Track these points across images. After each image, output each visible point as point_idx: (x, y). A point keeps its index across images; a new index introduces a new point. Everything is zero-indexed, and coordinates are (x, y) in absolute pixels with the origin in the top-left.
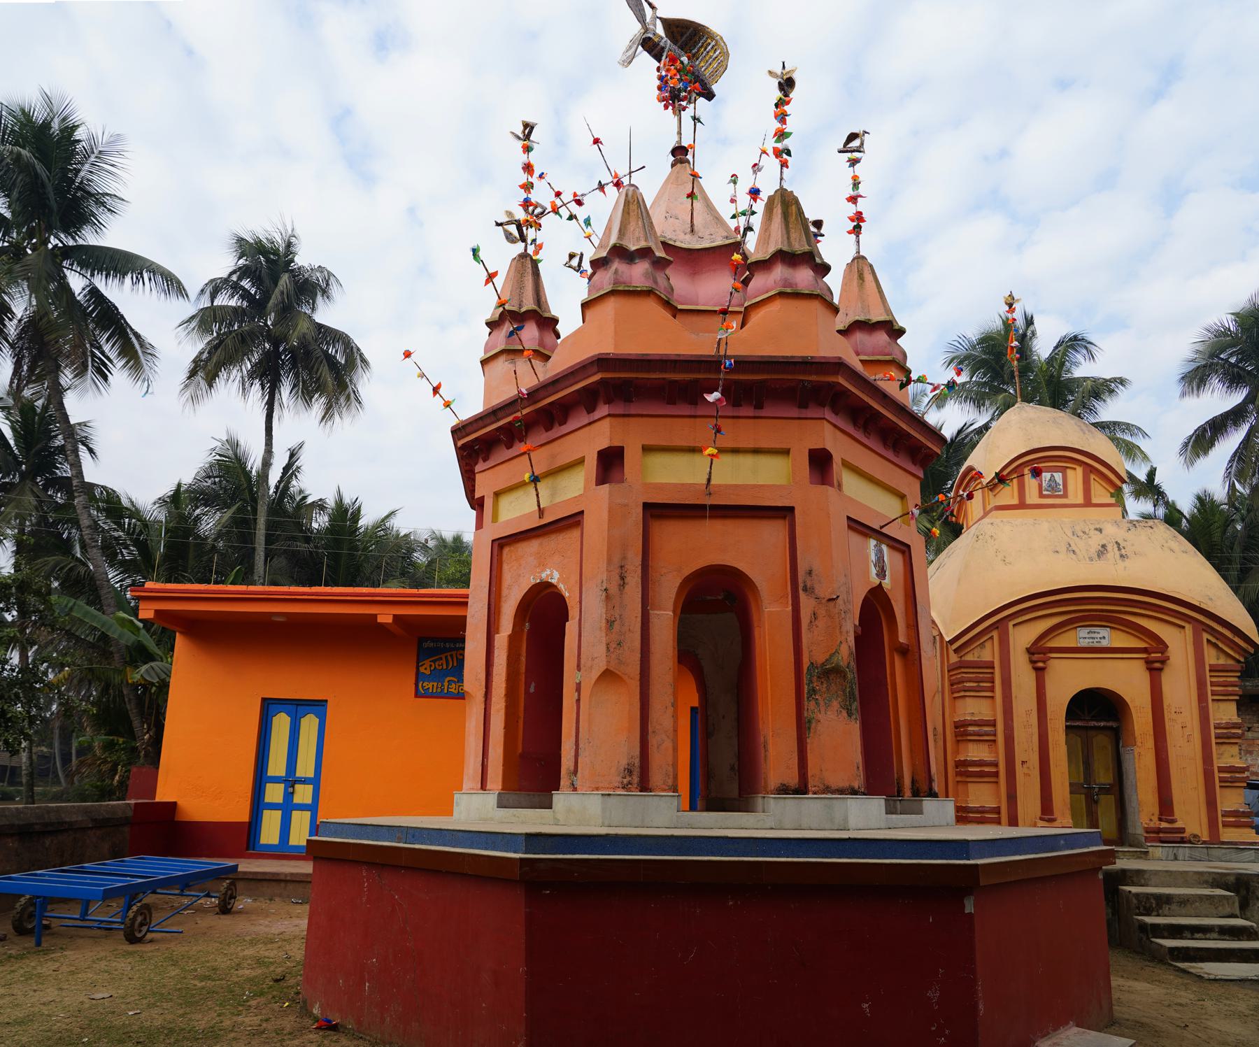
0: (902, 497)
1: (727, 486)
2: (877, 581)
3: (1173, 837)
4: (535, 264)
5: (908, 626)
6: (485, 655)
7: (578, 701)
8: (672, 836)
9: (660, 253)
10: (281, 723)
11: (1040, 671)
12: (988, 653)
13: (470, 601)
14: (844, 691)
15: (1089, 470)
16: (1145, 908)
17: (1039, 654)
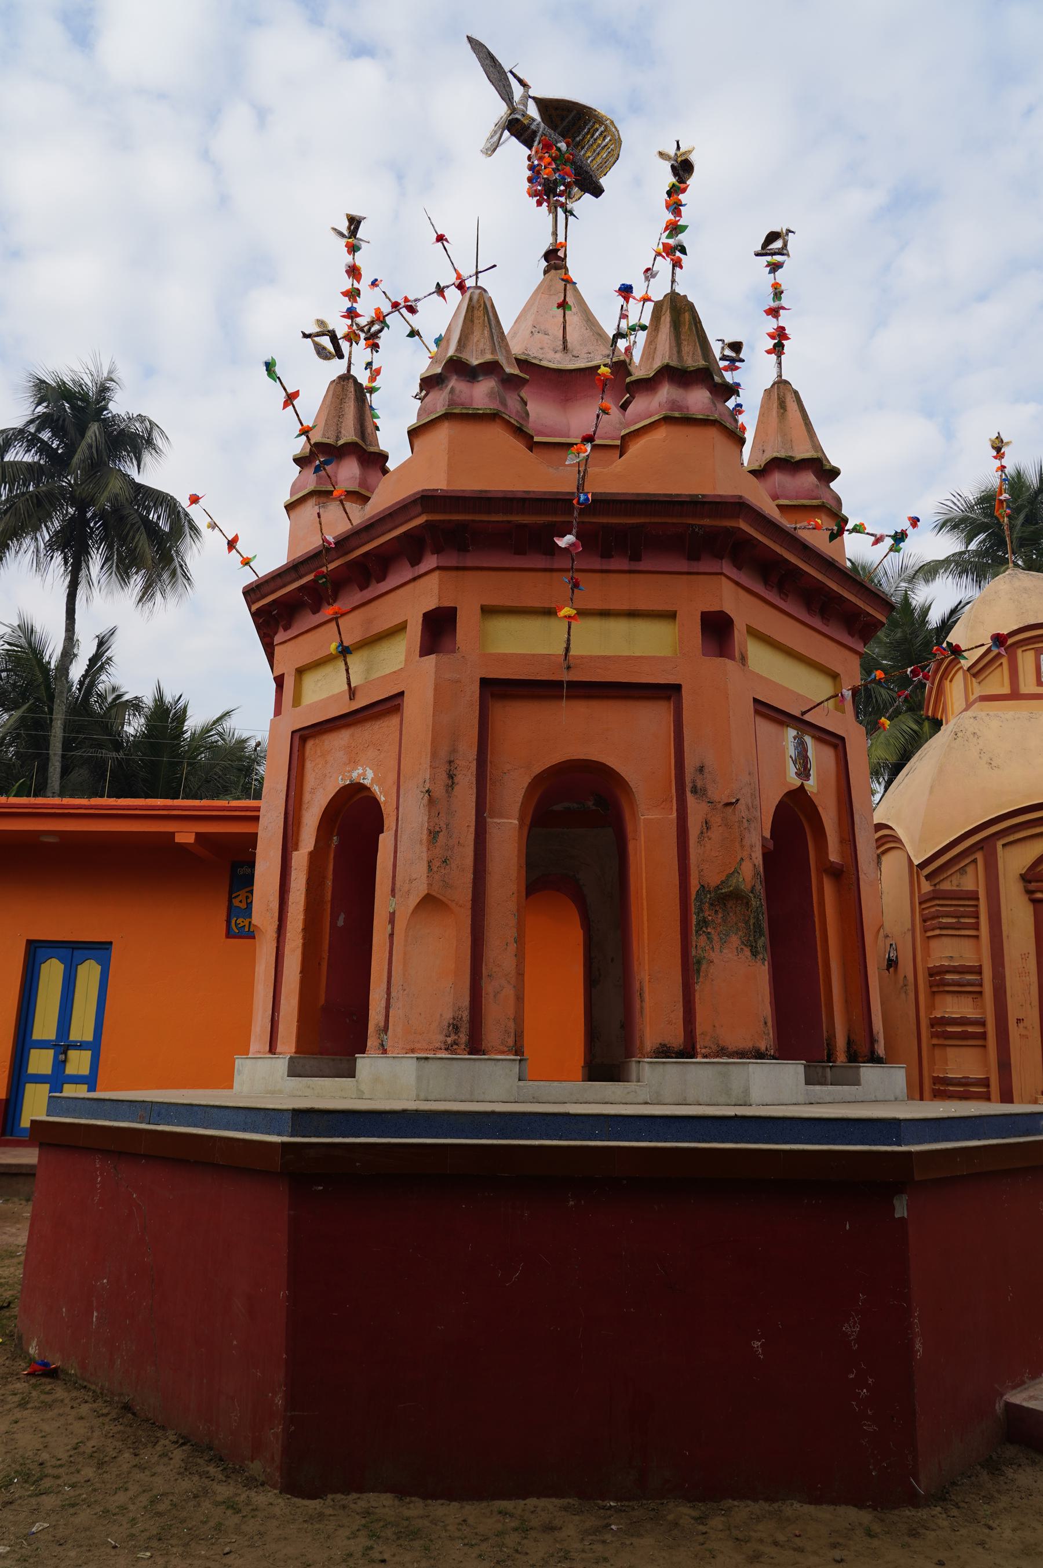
0: (834, 676)
1: (592, 658)
2: (797, 782)
4: (361, 393)
5: (842, 841)
6: (279, 881)
7: (392, 935)
8: (493, 1113)
9: (511, 369)
10: (52, 972)
13: (262, 813)
14: (747, 922)
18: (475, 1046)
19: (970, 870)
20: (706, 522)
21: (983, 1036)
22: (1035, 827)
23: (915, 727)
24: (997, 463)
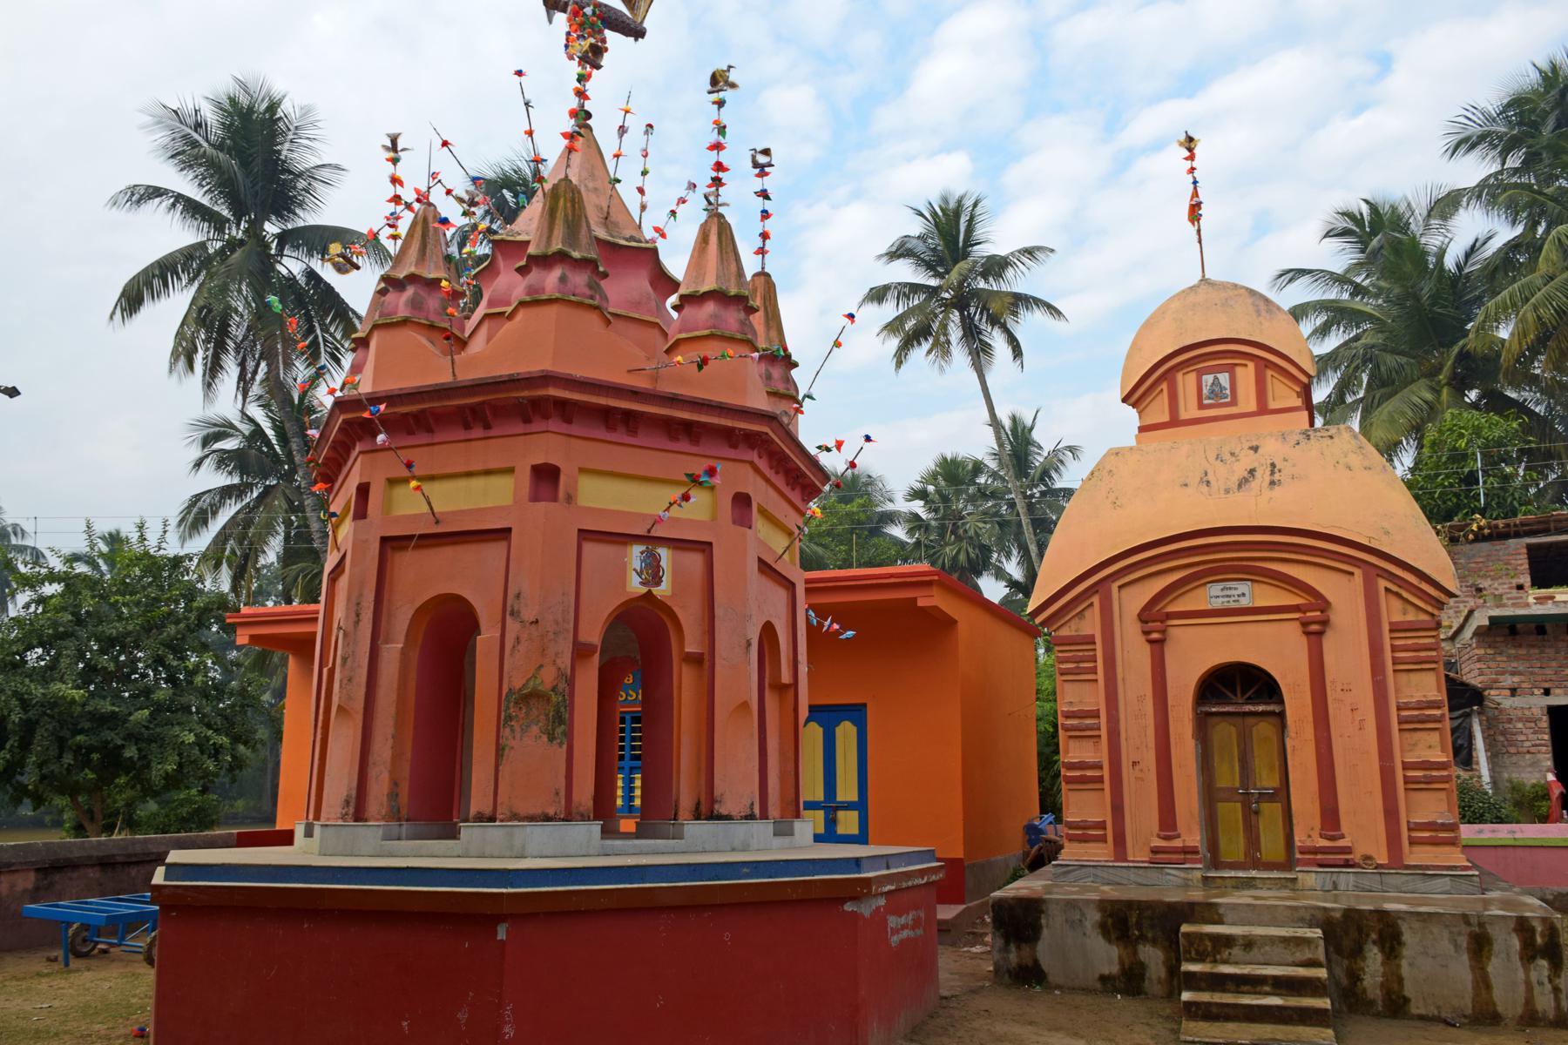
2: (644, 590)
11: (1158, 646)
12: (1090, 624)
15: (1263, 365)
16: (1197, 952)
17: (1154, 619)
18: (359, 815)
19: (1087, 613)
20: (526, 393)
21: (1100, 780)
23: (1429, 396)
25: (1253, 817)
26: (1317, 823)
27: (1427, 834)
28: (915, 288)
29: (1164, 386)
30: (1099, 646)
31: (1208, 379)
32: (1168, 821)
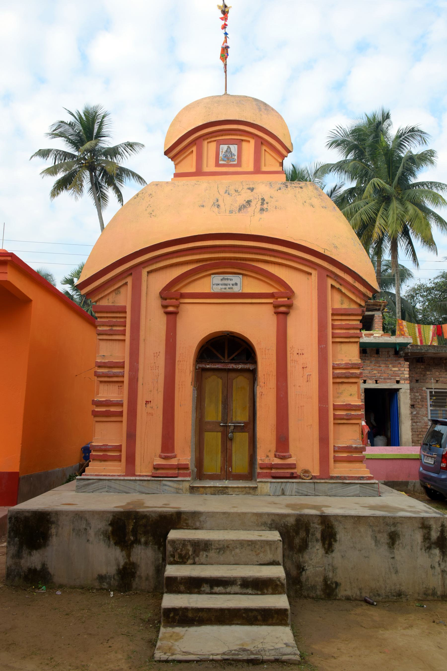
3: (285, 473)
11: (172, 316)
12: (123, 299)
16: (181, 556)
21: (120, 414)
22: (172, 258)
24: (223, 22)
25: (229, 443)
26: (273, 447)
27: (345, 455)
28: (66, 155)
29: (194, 149)
30: (128, 315)
31: (224, 148)
32: (168, 444)
